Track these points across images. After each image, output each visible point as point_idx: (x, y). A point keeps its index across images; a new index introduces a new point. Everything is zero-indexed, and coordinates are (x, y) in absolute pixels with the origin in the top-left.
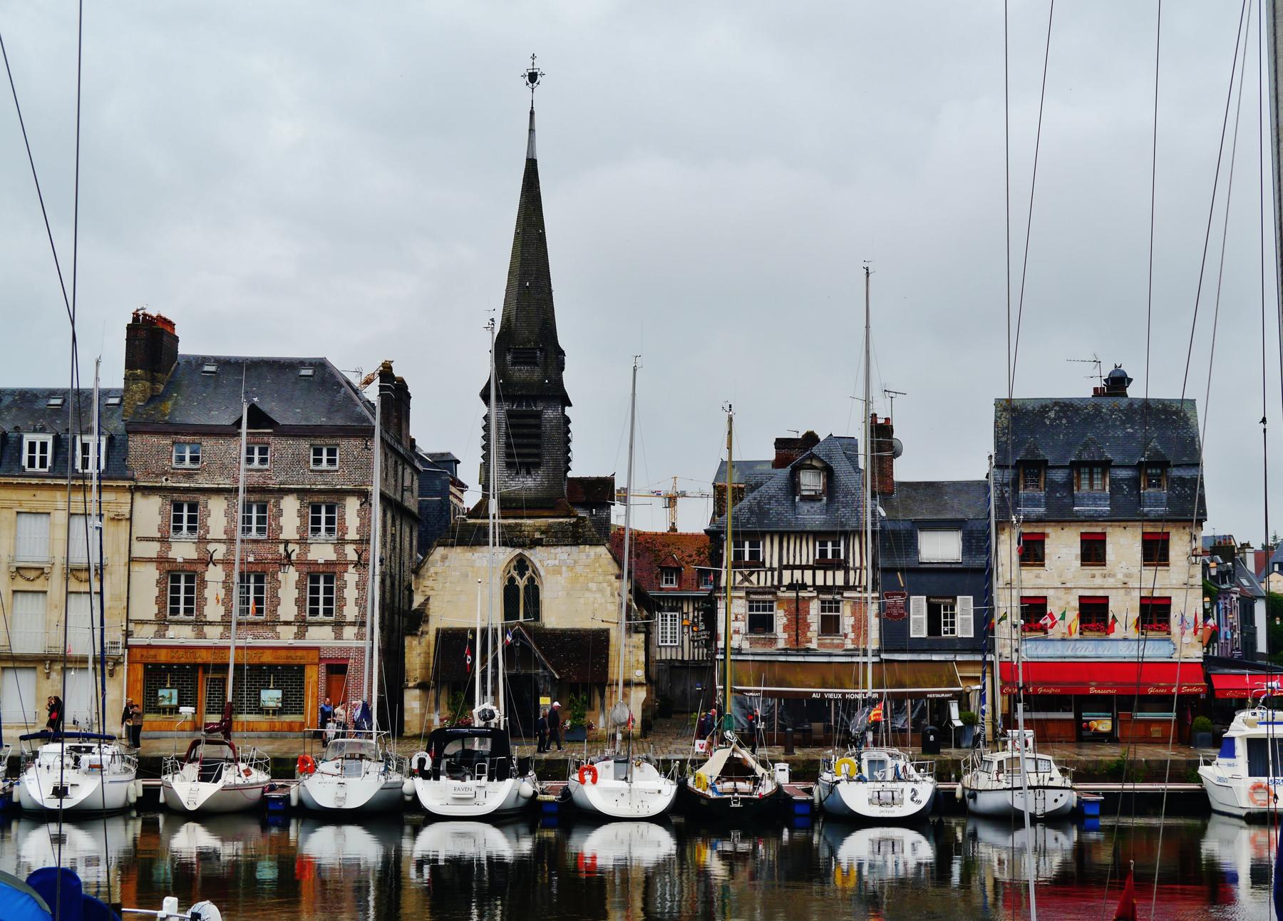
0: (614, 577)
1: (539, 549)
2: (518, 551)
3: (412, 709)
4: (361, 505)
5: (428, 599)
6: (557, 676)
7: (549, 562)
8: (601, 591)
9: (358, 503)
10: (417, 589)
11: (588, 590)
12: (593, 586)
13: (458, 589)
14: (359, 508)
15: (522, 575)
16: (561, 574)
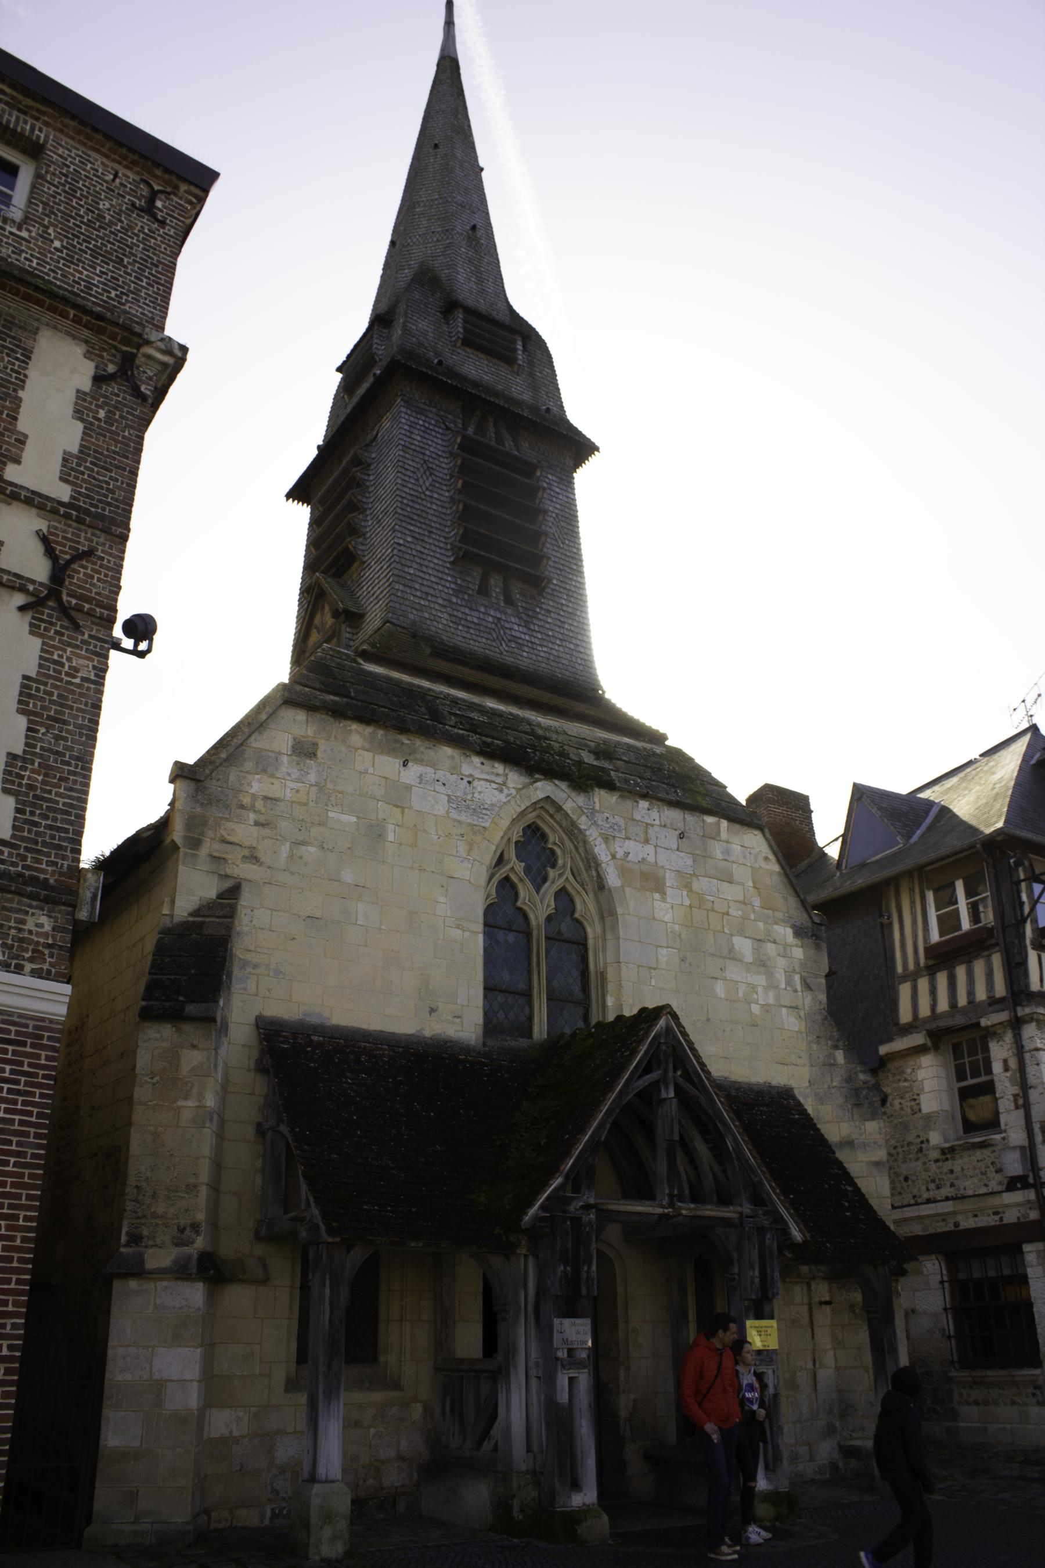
0: (789, 932)
1: (602, 798)
2: (543, 788)
3: (159, 1388)
4: (98, 379)
5: (232, 893)
6: (796, 1234)
7: (631, 846)
8: (762, 964)
9: (88, 368)
10: (195, 843)
11: (732, 955)
12: (744, 946)
13: (348, 876)
14: (86, 385)
15: (539, 880)
16: (663, 893)
